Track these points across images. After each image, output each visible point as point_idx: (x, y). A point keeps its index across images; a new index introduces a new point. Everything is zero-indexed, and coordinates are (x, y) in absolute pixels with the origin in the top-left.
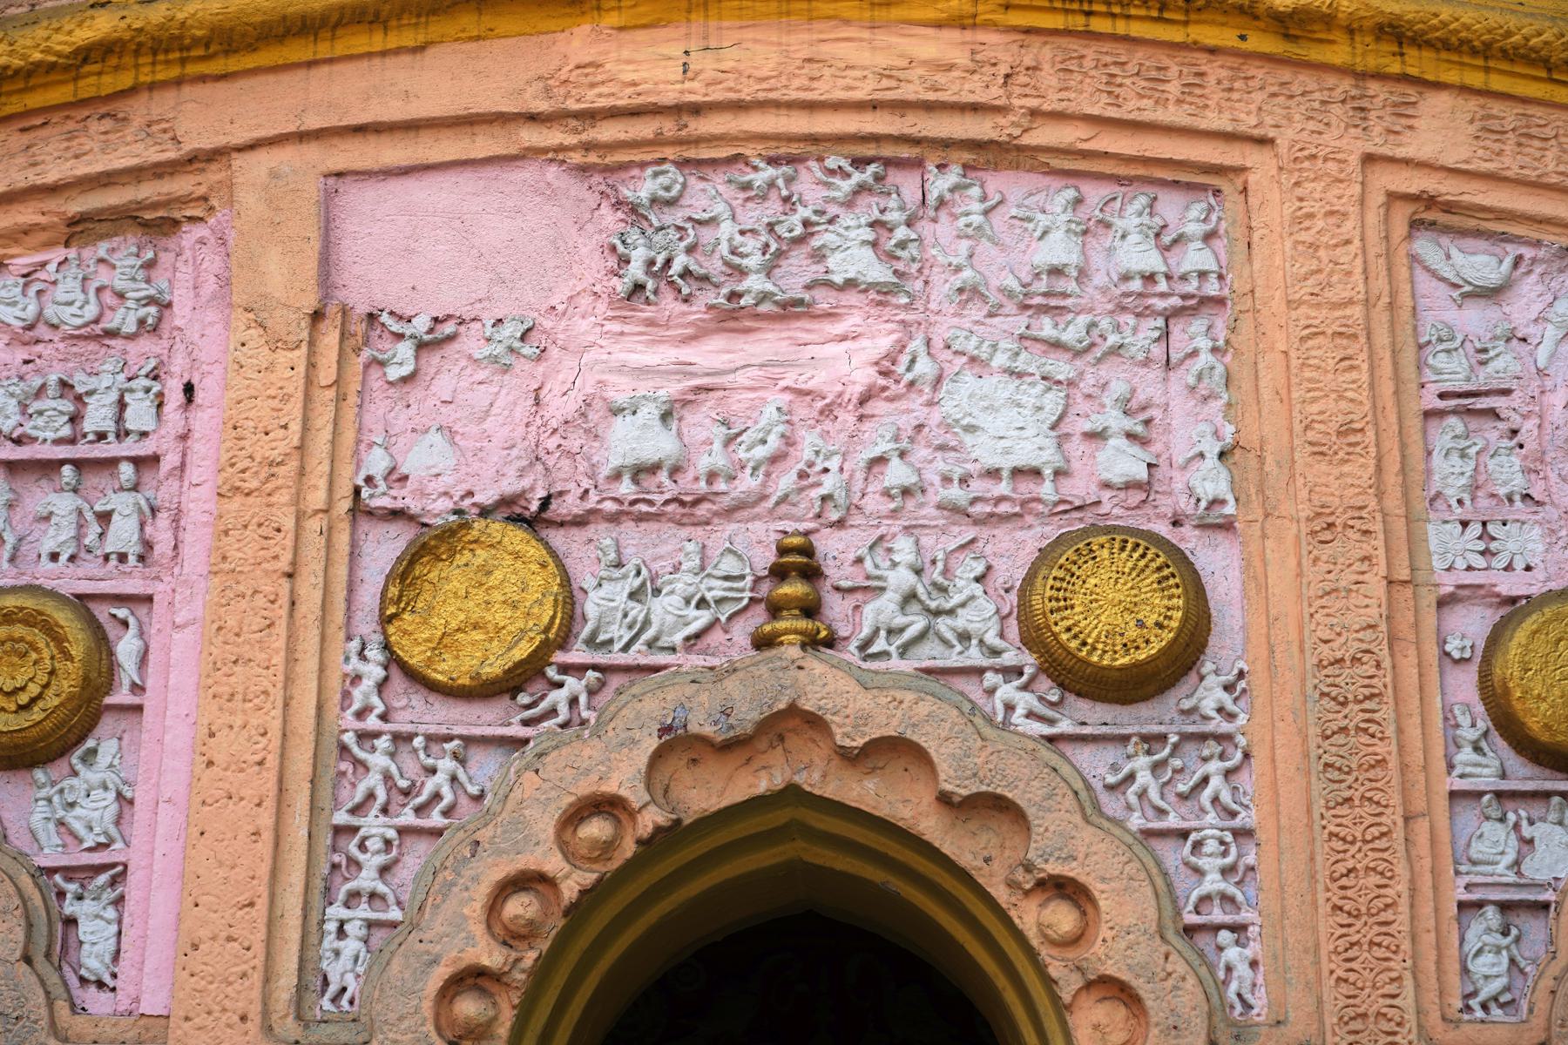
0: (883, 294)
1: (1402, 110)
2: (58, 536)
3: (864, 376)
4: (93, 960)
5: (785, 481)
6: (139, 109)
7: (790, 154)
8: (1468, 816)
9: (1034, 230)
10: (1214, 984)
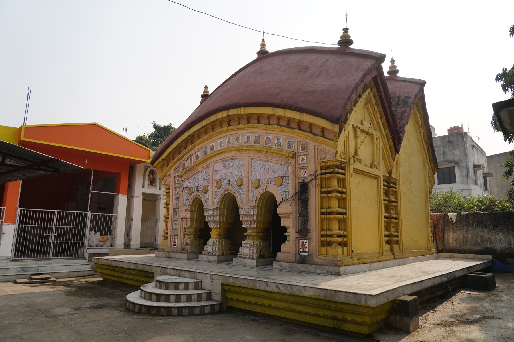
9: (237, 163)
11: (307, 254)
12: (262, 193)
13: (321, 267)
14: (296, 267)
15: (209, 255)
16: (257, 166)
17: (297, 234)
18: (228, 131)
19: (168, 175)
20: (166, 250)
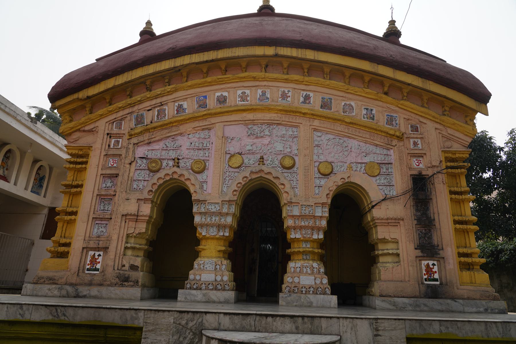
0: (269, 136)
1: (313, 121)
2: (202, 155)
3: (268, 143)
4: (205, 189)
5: (261, 151)
6: (208, 120)
7: (262, 124)
8: (316, 179)
10: (295, 192)
11: (438, 283)
14: (425, 305)
15: (207, 288)
16: (325, 142)
17: (417, 251)
18: (264, 79)
19: (87, 128)
20: (63, 281)
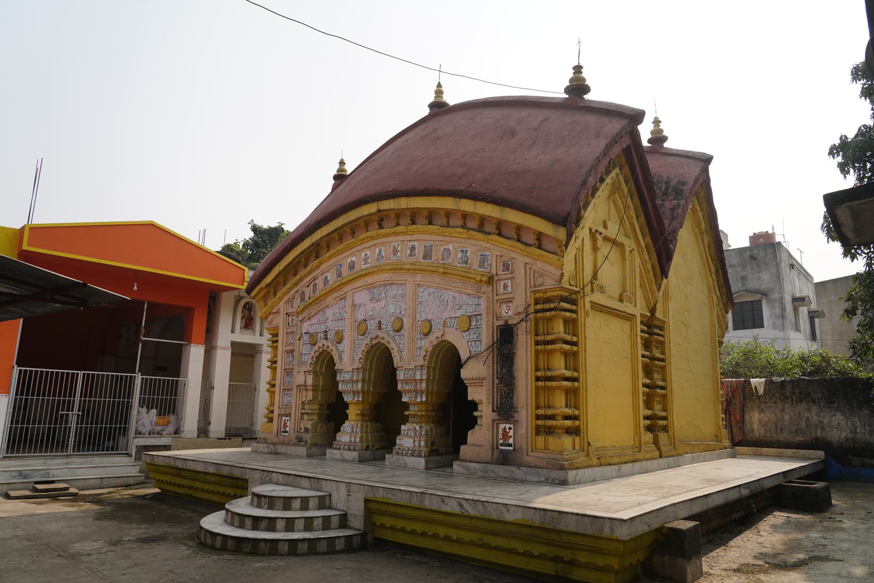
9: (394, 291)
11: (512, 448)
12: (435, 343)
13: (534, 470)
14: (493, 471)
15: (344, 449)
16: (427, 297)
17: (495, 414)
18: (379, 237)
19: (274, 311)
20: (269, 441)
